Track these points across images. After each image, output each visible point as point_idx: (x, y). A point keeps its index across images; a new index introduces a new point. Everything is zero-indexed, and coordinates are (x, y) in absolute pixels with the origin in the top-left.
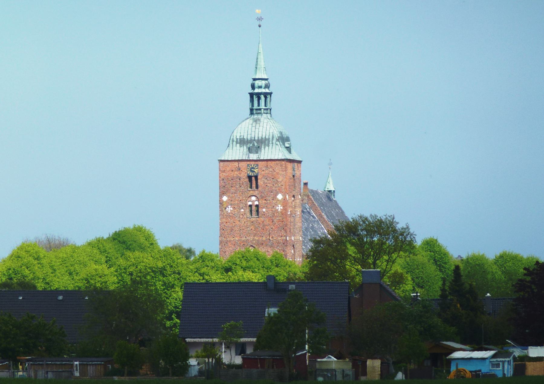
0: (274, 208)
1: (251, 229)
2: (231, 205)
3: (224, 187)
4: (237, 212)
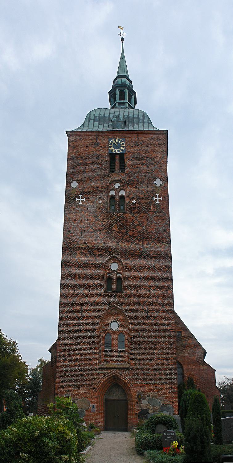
0: (149, 199)
1: (114, 230)
2: (83, 193)
3: (74, 168)
4: (91, 204)
